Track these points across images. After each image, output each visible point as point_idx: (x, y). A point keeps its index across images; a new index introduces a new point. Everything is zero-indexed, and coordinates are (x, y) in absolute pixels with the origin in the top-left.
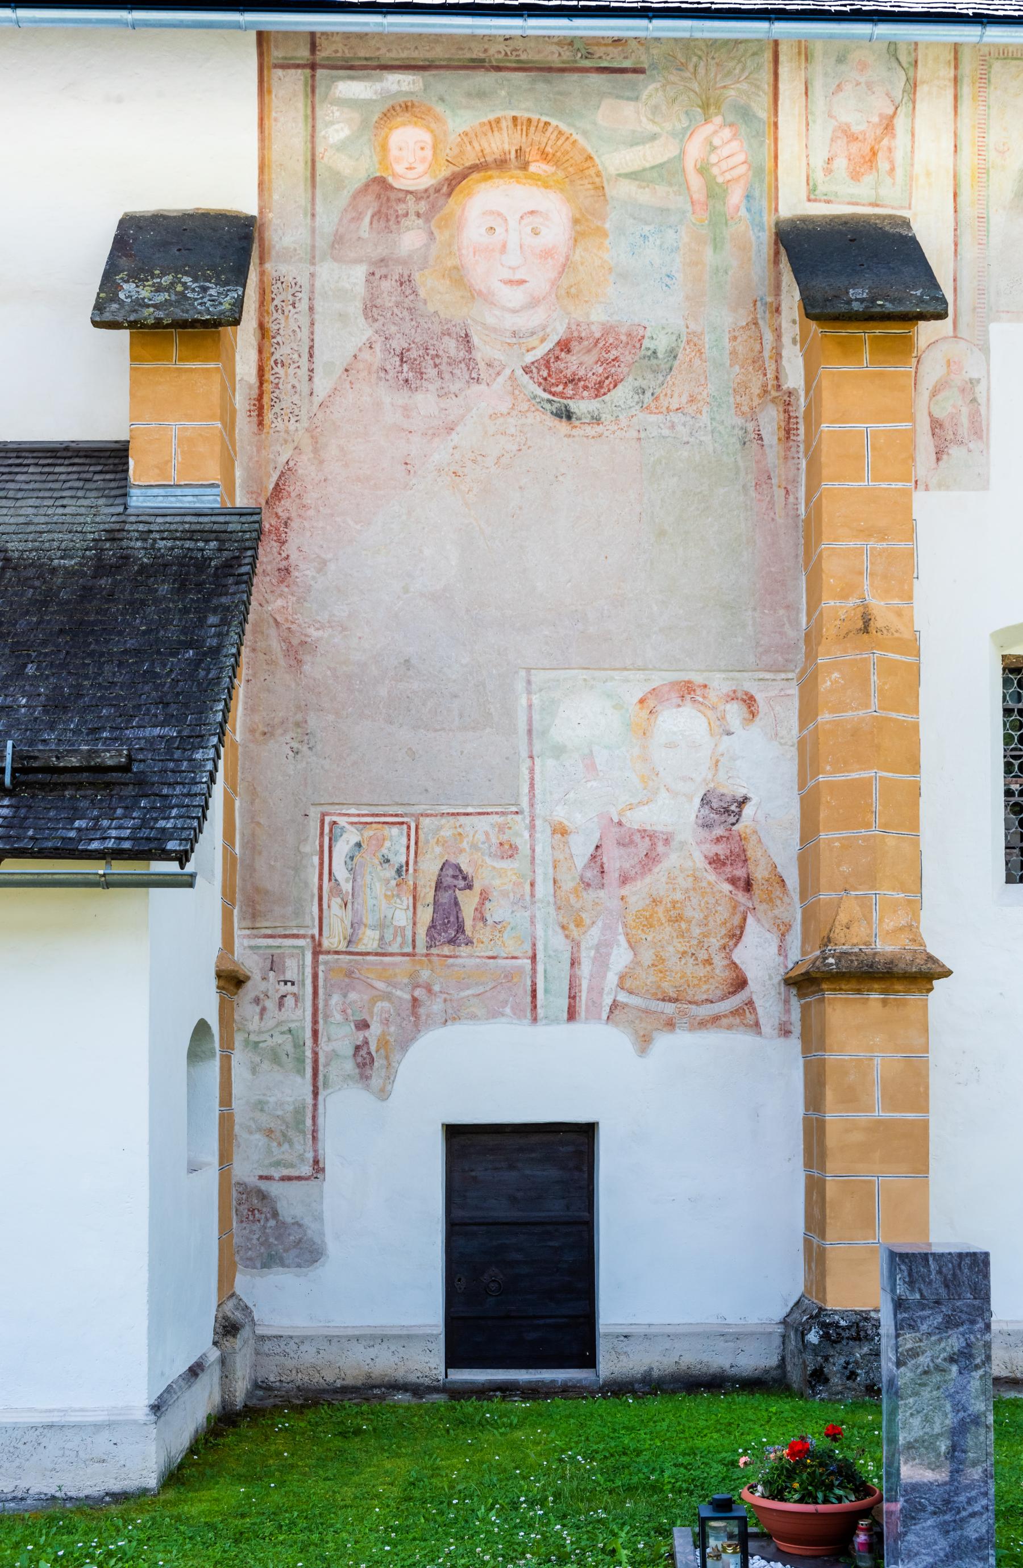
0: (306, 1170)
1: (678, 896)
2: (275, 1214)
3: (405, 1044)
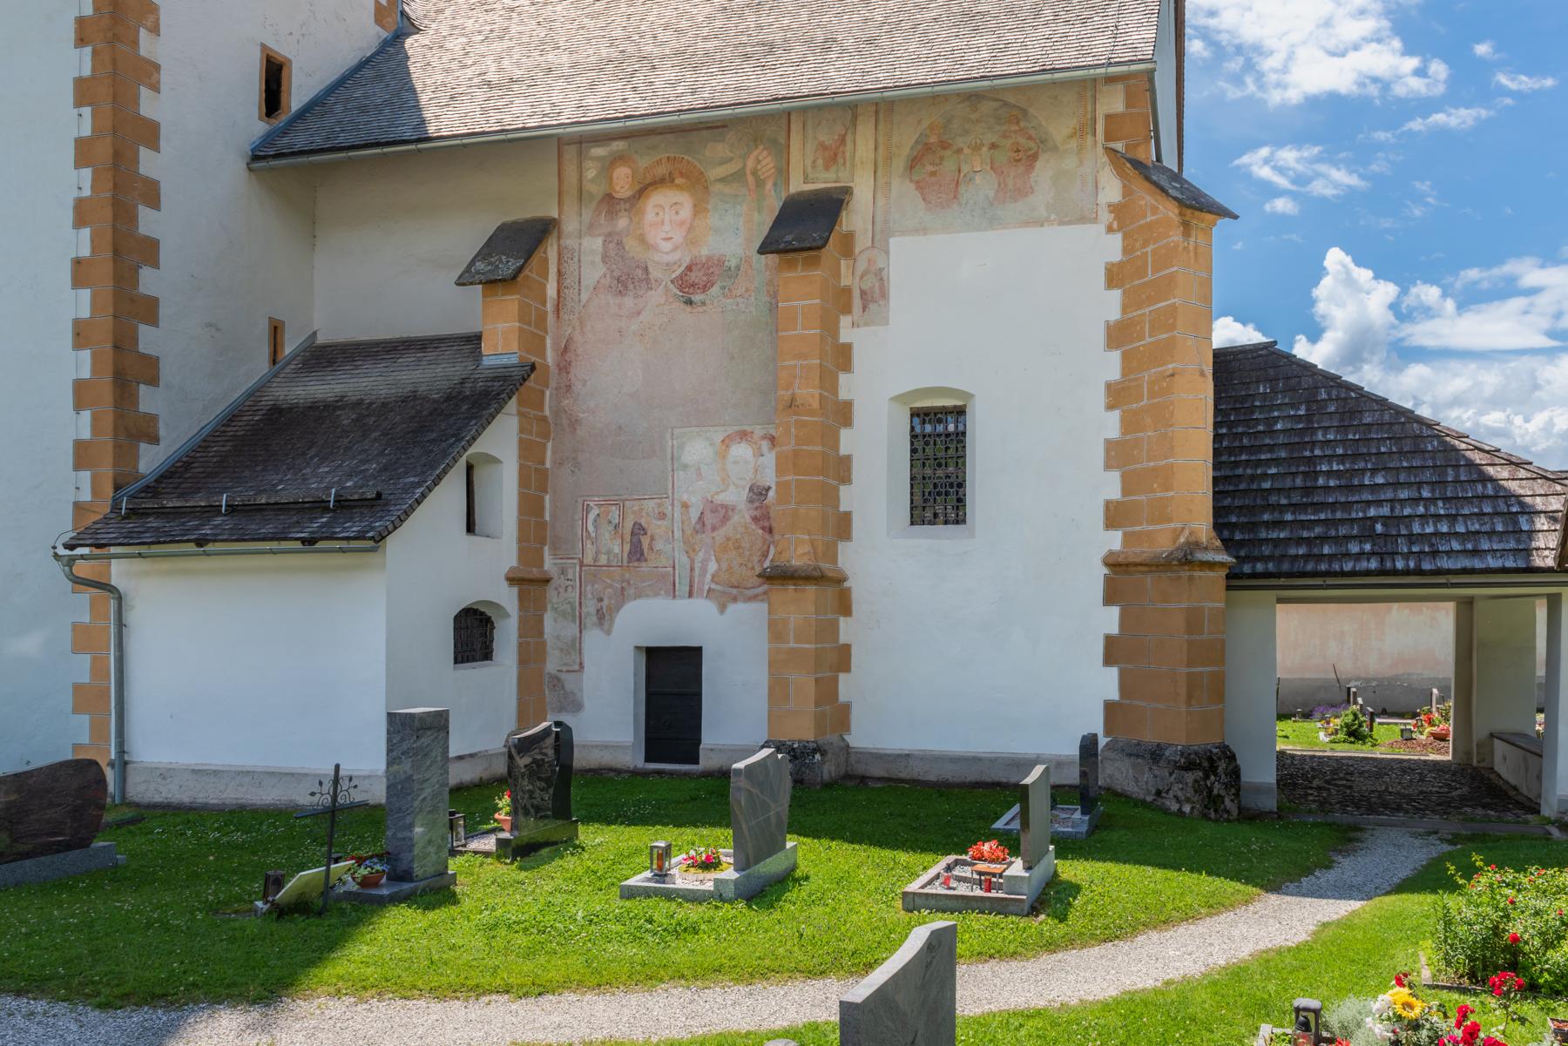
0: (576, 667)
1: (738, 536)
2: (563, 688)
3: (618, 609)
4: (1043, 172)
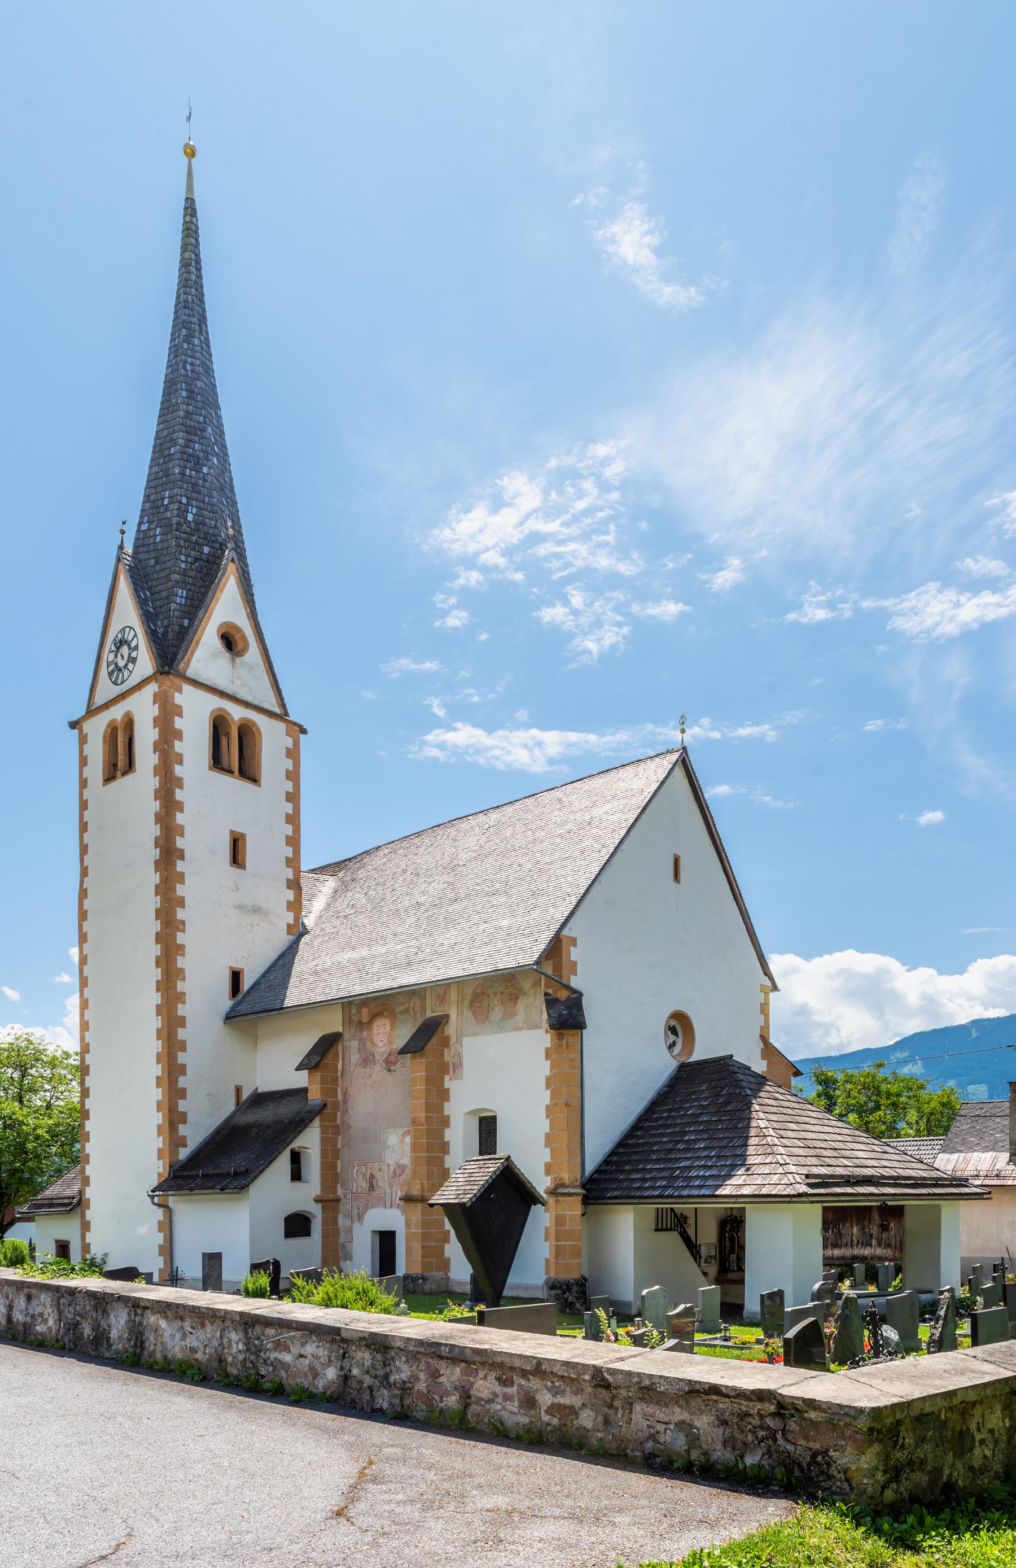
4: (521, 1005)
